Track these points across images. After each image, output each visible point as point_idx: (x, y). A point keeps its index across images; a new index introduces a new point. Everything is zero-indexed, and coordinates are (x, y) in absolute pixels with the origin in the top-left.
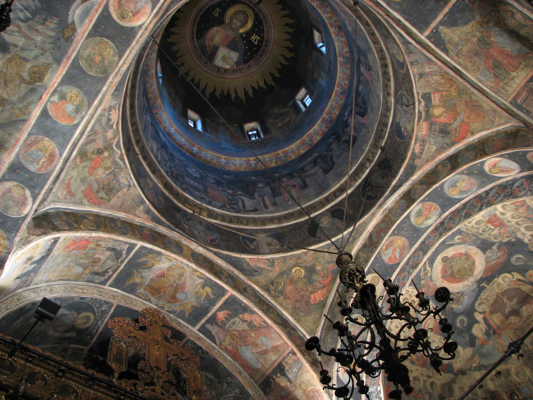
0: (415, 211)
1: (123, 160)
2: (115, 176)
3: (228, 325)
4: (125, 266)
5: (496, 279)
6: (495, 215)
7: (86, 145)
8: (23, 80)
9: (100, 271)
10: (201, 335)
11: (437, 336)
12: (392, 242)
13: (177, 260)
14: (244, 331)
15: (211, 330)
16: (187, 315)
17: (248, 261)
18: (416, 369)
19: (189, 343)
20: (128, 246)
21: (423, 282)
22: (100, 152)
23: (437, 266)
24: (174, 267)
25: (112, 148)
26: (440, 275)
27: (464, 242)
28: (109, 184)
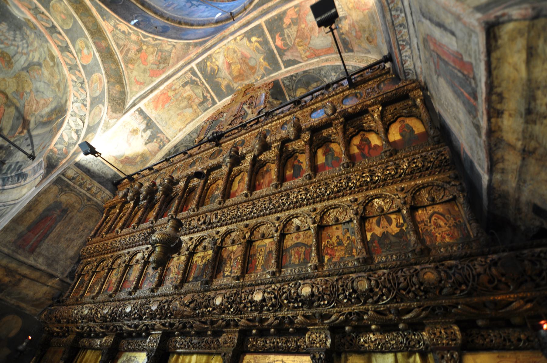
1: (156, 39)
2: (161, 51)
3: (289, 43)
4: (208, 83)
7: (127, 56)
8: (53, 67)
9: (201, 100)
13: (221, 47)
14: (297, 32)
15: (288, 58)
16: (269, 68)
19: (285, 81)
20: (190, 73)
22: (139, 50)
24: (225, 53)
25: (144, 42)
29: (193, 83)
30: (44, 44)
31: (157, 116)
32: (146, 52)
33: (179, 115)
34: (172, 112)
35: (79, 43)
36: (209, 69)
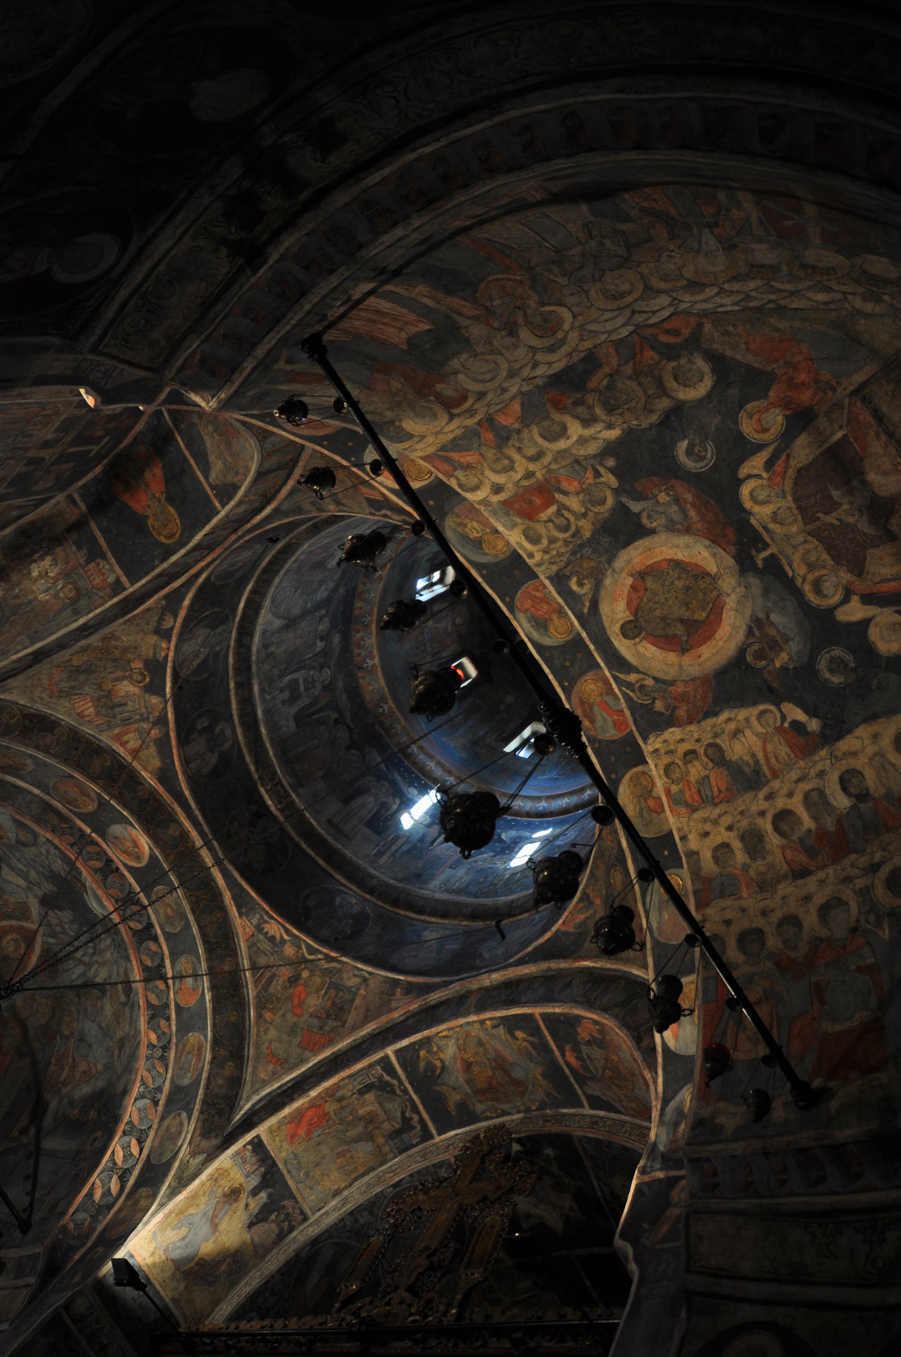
0: (531, 629)
2: (337, 987)
4: (416, 1093)
5: (753, 521)
6: (505, 503)
7: (265, 988)
8: (124, 1005)
10: (601, 1113)
11: (816, 758)
12: (582, 703)
13: (452, 1029)
17: (563, 929)
18: (822, 882)
20: (379, 1068)
21: (659, 706)
22: (294, 980)
23: (639, 655)
26: (672, 657)
27: (597, 577)
28: (334, 1004)
29: (383, 1088)
30: (122, 961)
31: (291, 1156)
32: (306, 985)
33: (339, 1155)
34: (325, 1149)
35: (184, 964)
36: (422, 1064)
